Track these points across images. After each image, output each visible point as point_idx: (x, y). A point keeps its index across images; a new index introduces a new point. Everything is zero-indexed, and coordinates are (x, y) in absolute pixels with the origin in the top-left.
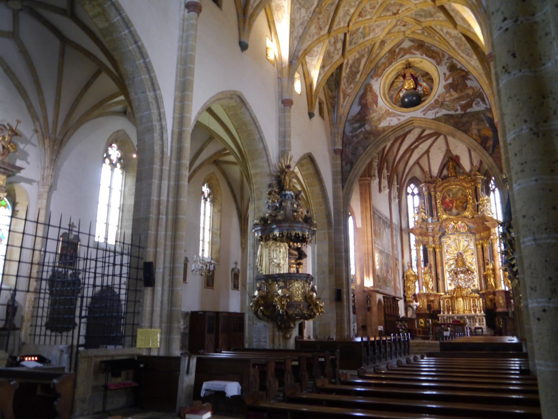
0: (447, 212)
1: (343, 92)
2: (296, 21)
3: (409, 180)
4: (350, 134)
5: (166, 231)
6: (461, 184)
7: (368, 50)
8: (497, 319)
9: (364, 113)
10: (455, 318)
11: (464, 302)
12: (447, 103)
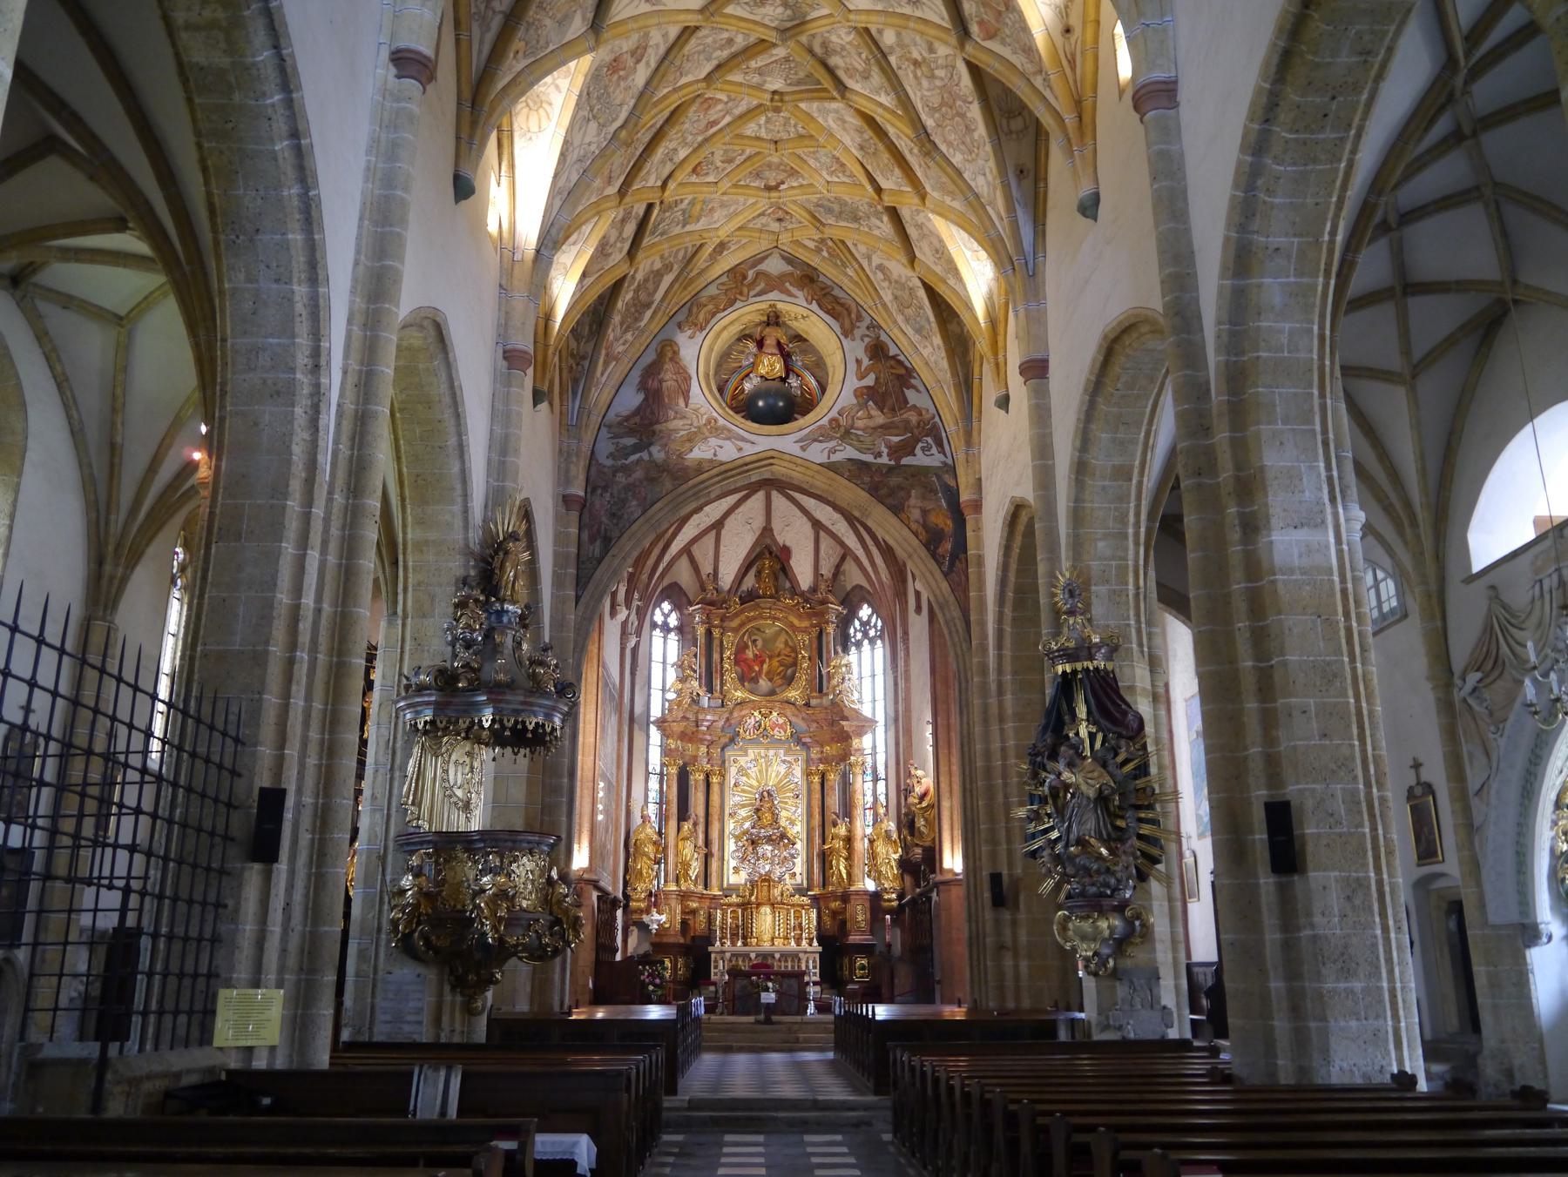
1: (607, 349)
3: (662, 591)
4: (609, 462)
5: (309, 698)
7: (684, 258)
8: (846, 961)
9: (653, 413)
10: (753, 956)
12: (860, 433)
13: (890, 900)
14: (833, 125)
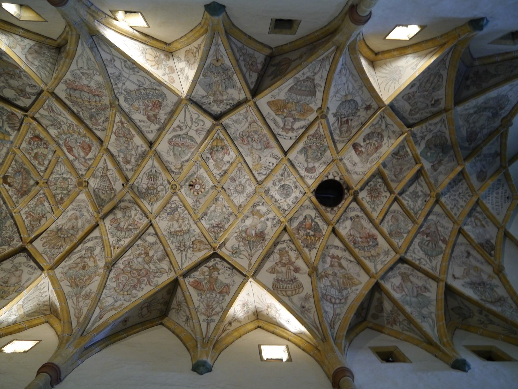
2: (131, 73)
14: (70, 213)
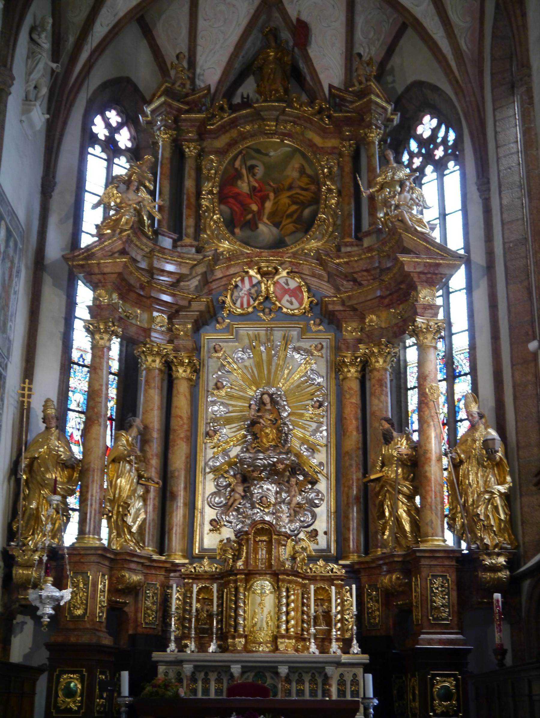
0: (237, 230)
6: (302, 134)
8: (414, 682)
10: (236, 669)
11: (279, 598)
13: (494, 568)
